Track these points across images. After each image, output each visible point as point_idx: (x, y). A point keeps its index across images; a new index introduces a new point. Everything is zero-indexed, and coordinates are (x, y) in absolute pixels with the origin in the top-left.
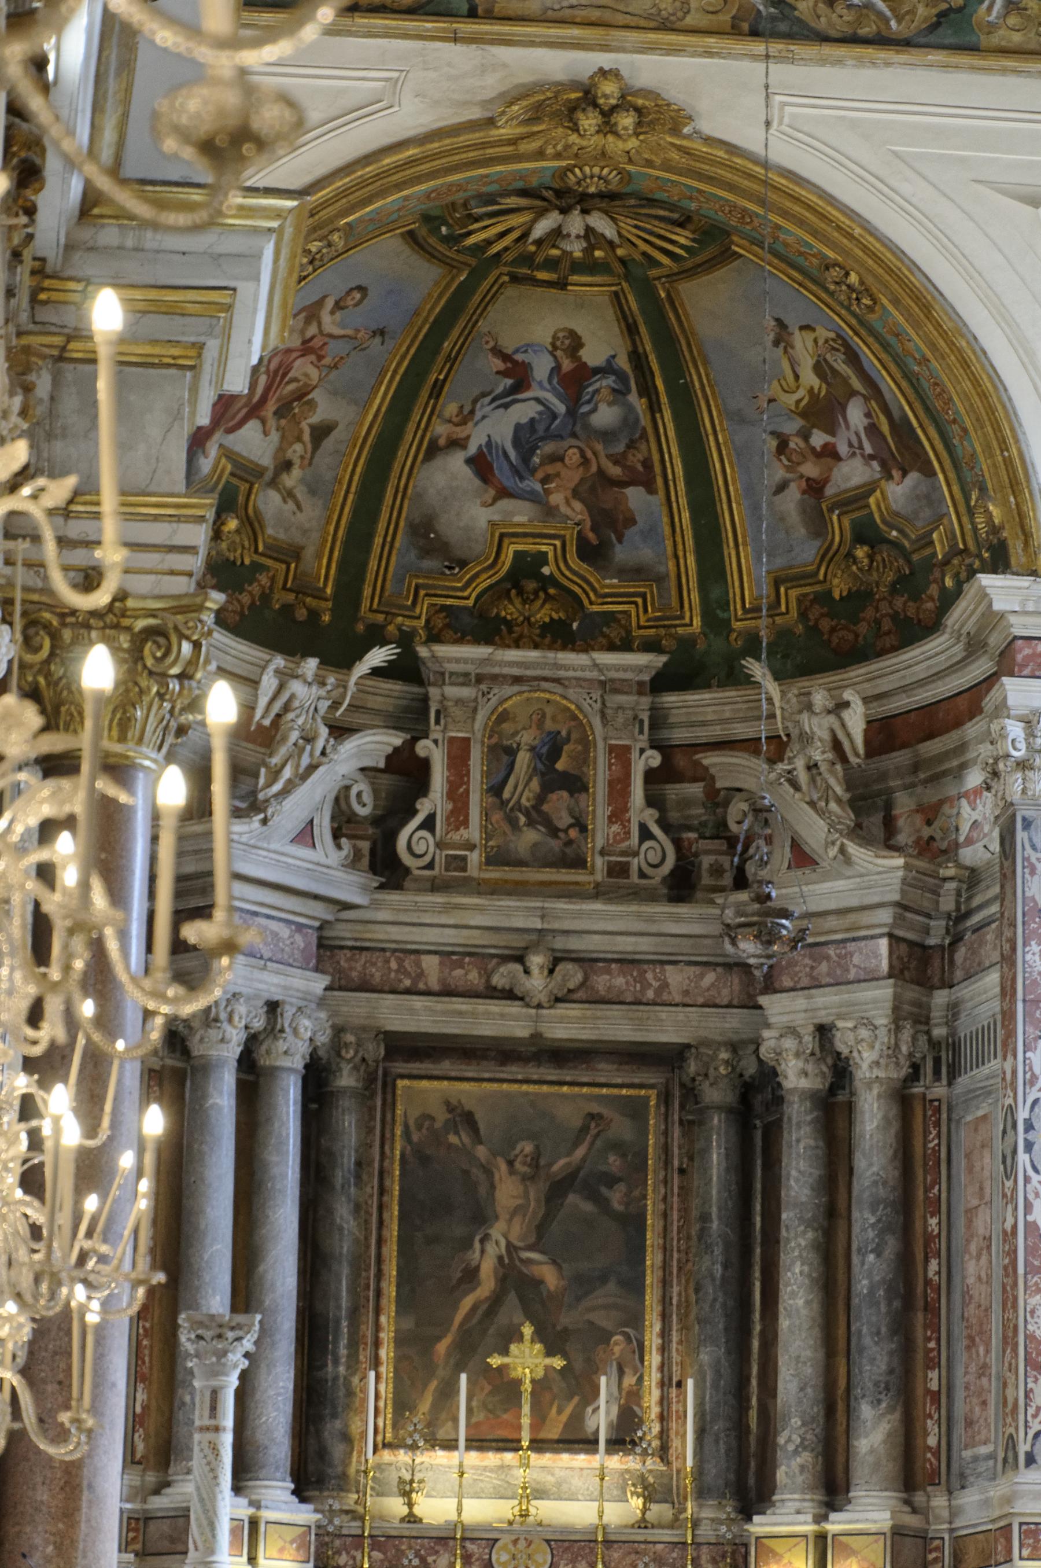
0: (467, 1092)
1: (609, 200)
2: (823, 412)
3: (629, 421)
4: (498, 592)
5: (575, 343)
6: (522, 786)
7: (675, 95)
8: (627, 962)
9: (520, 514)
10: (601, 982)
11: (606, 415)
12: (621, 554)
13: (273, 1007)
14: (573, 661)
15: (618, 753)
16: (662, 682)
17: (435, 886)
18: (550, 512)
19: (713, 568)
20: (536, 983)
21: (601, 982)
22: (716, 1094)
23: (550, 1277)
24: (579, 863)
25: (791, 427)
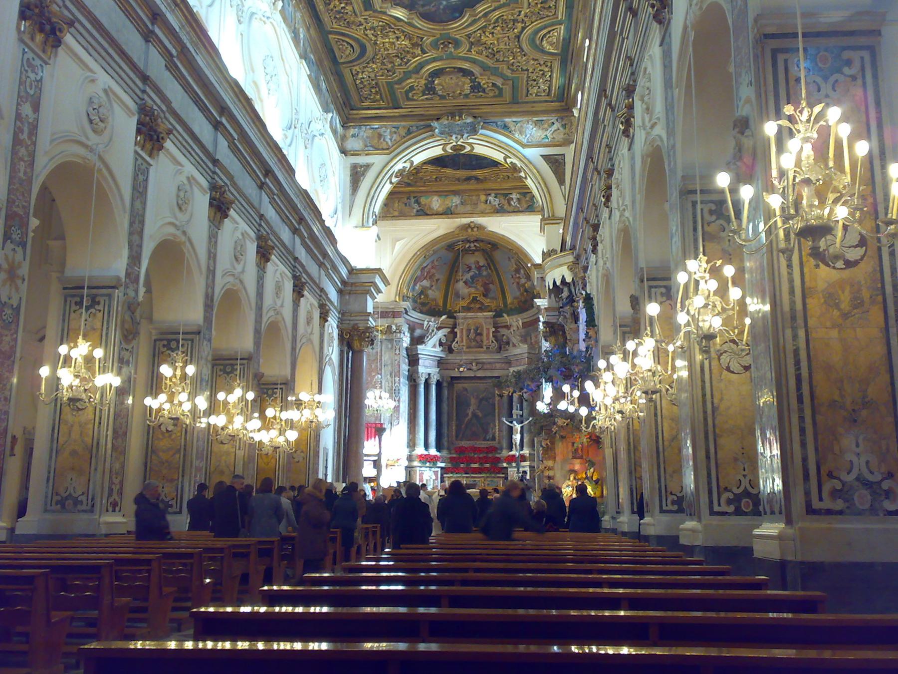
0: (466, 385)
1: (476, 241)
2: (517, 271)
3: (489, 274)
4: (470, 303)
6: (472, 335)
8: (490, 363)
9: (473, 290)
10: (485, 367)
11: (485, 273)
12: (490, 295)
13: (429, 374)
15: (489, 330)
16: (494, 316)
17: (458, 353)
18: (477, 289)
20: (474, 368)
21: (485, 367)
23: (480, 414)
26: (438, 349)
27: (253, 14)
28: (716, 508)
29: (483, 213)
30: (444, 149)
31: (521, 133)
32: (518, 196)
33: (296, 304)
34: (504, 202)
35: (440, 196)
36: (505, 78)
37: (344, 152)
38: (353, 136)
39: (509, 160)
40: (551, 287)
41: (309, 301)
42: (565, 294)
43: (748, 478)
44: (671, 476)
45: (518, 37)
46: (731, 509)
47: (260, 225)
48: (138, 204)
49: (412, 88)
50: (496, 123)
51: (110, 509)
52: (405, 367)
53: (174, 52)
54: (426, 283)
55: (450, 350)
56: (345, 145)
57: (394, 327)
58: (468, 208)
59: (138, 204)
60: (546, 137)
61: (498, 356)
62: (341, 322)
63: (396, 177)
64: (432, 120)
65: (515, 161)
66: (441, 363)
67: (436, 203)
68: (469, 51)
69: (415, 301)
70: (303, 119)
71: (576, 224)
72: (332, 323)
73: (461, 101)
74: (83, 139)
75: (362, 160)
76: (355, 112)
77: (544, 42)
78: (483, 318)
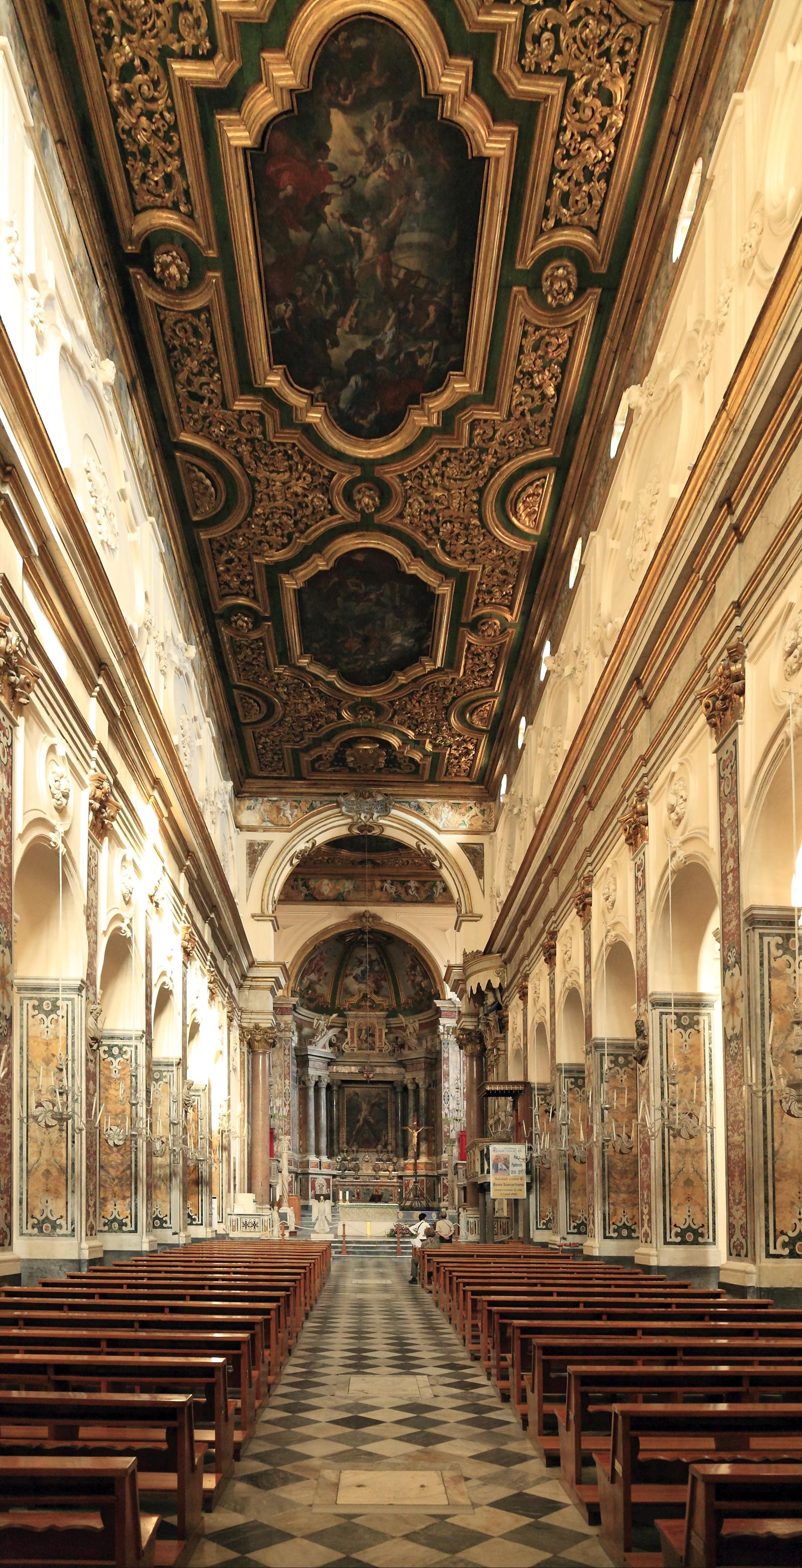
2: (413, 968)
9: (363, 986)
16: (387, 1017)
29: (378, 902)
32: (417, 884)
34: (401, 890)
35: (330, 880)
36: (426, 755)
38: (249, 808)
49: (320, 758)
50: (409, 803)
58: (362, 895)
68: (391, 719)
78: (375, 1018)
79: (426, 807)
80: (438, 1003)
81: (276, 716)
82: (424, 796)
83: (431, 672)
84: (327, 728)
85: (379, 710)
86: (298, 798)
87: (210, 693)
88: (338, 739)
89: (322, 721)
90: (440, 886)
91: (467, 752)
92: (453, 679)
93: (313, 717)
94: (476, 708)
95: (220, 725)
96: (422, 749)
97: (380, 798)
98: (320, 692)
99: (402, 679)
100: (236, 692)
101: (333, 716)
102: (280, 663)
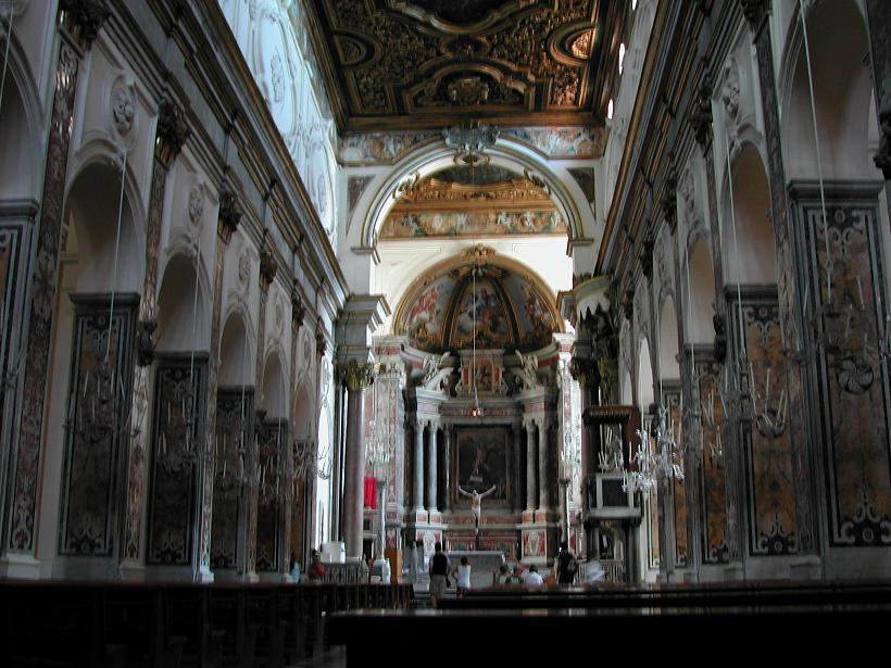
2: (532, 301)
5: (485, 292)
6: (479, 376)
7: (493, 247)
11: (493, 304)
12: (499, 330)
14: (487, 352)
16: (505, 355)
19: (516, 331)
22: (517, 432)
24: (489, 389)
25: (527, 304)
26: (440, 392)
27: (263, 11)
28: (836, 539)
29: (492, 235)
30: (455, 160)
31: (544, 144)
32: (533, 215)
33: (295, 333)
34: (517, 222)
35: (443, 215)
37: (341, 163)
39: (530, 174)
40: (584, 317)
41: (307, 328)
42: (601, 323)
43: (869, 506)
44: (762, 516)
45: (546, 40)
46: (852, 540)
47: (264, 241)
48: (155, 214)
49: (421, 94)
51: (129, 554)
52: (401, 413)
53: (195, 48)
54: (424, 315)
55: (453, 394)
56: (342, 155)
57: (388, 367)
58: (476, 229)
59: (155, 214)
60: (572, 149)
61: (507, 401)
62: (337, 356)
63: (400, 190)
64: (441, 128)
65: (538, 174)
66: (442, 408)
67: (438, 222)
68: (491, 54)
69: (412, 336)
70: (306, 123)
71: (617, 243)
72: (328, 356)
73: (478, 107)
74: (109, 139)
75: (362, 172)
76: (354, 119)
77: (574, 46)
79: (533, 137)
80: (557, 337)
81: (375, 56)
82: (531, 125)
83: (525, 9)
84: (426, 66)
85: (478, 46)
86: (402, 133)
87: (309, 37)
88: (438, 75)
89: (422, 59)
90: (558, 217)
91: (571, 81)
92: (549, 15)
93: (411, 56)
94: (575, 39)
95: (320, 68)
96: (525, 80)
97: (484, 129)
98: (417, 32)
99: (497, 16)
100: (336, 39)
101: (432, 53)
102: (378, 8)
